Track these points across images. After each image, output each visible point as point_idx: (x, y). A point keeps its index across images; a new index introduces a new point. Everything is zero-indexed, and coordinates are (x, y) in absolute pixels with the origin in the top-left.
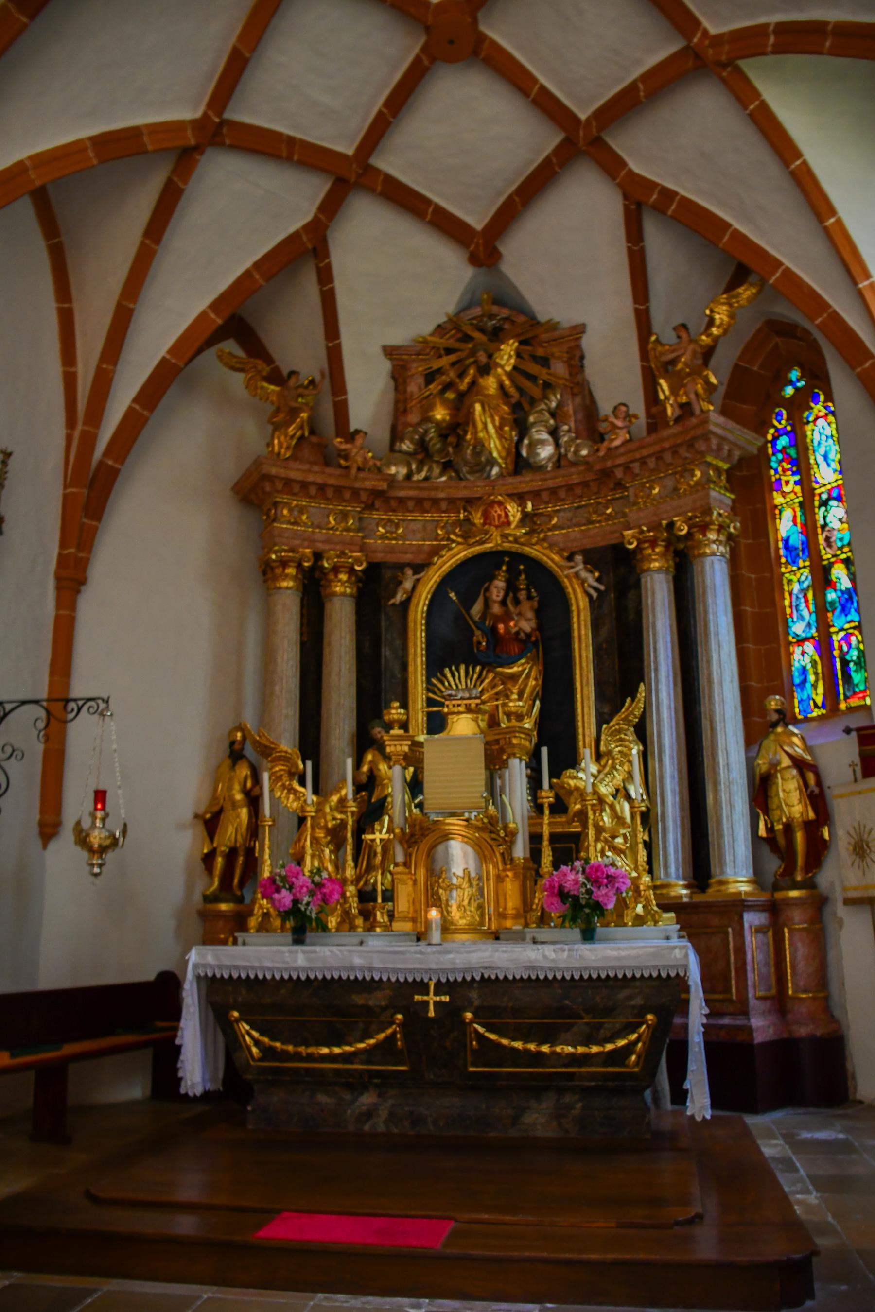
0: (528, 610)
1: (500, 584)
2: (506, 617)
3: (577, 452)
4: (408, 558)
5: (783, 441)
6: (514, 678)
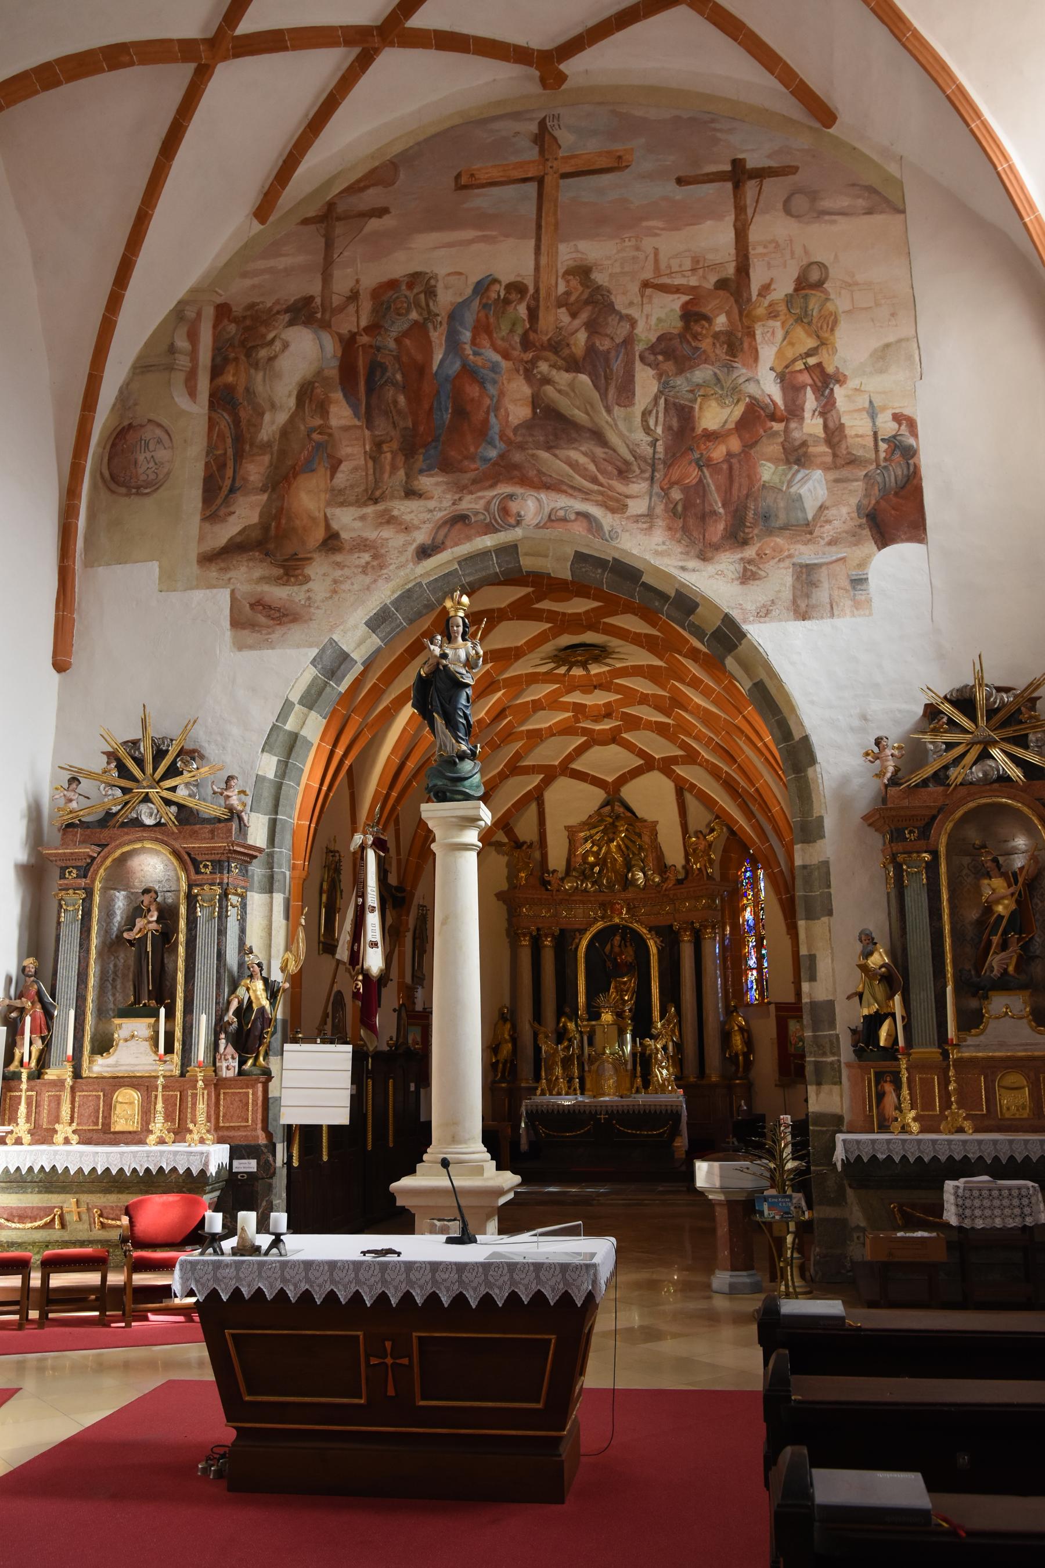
0: (630, 951)
1: (618, 938)
2: (621, 953)
3: (653, 881)
4: (577, 926)
5: (748, 874)
6: (625, 983)
